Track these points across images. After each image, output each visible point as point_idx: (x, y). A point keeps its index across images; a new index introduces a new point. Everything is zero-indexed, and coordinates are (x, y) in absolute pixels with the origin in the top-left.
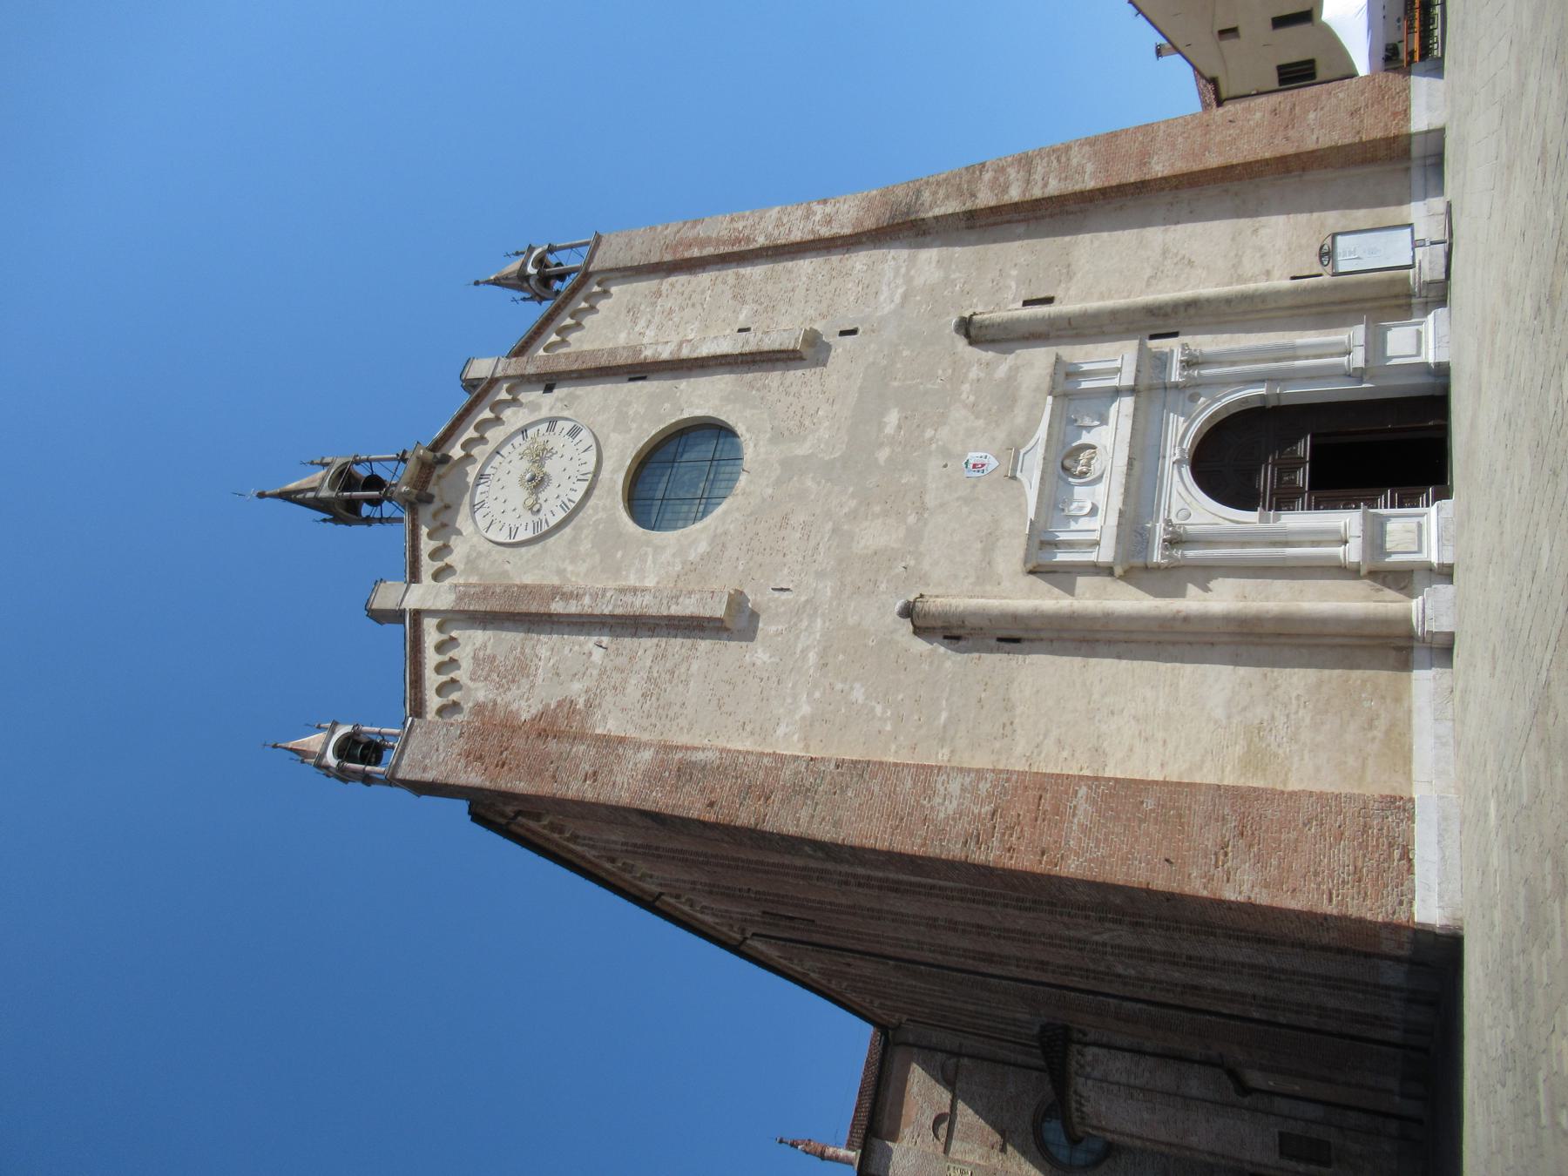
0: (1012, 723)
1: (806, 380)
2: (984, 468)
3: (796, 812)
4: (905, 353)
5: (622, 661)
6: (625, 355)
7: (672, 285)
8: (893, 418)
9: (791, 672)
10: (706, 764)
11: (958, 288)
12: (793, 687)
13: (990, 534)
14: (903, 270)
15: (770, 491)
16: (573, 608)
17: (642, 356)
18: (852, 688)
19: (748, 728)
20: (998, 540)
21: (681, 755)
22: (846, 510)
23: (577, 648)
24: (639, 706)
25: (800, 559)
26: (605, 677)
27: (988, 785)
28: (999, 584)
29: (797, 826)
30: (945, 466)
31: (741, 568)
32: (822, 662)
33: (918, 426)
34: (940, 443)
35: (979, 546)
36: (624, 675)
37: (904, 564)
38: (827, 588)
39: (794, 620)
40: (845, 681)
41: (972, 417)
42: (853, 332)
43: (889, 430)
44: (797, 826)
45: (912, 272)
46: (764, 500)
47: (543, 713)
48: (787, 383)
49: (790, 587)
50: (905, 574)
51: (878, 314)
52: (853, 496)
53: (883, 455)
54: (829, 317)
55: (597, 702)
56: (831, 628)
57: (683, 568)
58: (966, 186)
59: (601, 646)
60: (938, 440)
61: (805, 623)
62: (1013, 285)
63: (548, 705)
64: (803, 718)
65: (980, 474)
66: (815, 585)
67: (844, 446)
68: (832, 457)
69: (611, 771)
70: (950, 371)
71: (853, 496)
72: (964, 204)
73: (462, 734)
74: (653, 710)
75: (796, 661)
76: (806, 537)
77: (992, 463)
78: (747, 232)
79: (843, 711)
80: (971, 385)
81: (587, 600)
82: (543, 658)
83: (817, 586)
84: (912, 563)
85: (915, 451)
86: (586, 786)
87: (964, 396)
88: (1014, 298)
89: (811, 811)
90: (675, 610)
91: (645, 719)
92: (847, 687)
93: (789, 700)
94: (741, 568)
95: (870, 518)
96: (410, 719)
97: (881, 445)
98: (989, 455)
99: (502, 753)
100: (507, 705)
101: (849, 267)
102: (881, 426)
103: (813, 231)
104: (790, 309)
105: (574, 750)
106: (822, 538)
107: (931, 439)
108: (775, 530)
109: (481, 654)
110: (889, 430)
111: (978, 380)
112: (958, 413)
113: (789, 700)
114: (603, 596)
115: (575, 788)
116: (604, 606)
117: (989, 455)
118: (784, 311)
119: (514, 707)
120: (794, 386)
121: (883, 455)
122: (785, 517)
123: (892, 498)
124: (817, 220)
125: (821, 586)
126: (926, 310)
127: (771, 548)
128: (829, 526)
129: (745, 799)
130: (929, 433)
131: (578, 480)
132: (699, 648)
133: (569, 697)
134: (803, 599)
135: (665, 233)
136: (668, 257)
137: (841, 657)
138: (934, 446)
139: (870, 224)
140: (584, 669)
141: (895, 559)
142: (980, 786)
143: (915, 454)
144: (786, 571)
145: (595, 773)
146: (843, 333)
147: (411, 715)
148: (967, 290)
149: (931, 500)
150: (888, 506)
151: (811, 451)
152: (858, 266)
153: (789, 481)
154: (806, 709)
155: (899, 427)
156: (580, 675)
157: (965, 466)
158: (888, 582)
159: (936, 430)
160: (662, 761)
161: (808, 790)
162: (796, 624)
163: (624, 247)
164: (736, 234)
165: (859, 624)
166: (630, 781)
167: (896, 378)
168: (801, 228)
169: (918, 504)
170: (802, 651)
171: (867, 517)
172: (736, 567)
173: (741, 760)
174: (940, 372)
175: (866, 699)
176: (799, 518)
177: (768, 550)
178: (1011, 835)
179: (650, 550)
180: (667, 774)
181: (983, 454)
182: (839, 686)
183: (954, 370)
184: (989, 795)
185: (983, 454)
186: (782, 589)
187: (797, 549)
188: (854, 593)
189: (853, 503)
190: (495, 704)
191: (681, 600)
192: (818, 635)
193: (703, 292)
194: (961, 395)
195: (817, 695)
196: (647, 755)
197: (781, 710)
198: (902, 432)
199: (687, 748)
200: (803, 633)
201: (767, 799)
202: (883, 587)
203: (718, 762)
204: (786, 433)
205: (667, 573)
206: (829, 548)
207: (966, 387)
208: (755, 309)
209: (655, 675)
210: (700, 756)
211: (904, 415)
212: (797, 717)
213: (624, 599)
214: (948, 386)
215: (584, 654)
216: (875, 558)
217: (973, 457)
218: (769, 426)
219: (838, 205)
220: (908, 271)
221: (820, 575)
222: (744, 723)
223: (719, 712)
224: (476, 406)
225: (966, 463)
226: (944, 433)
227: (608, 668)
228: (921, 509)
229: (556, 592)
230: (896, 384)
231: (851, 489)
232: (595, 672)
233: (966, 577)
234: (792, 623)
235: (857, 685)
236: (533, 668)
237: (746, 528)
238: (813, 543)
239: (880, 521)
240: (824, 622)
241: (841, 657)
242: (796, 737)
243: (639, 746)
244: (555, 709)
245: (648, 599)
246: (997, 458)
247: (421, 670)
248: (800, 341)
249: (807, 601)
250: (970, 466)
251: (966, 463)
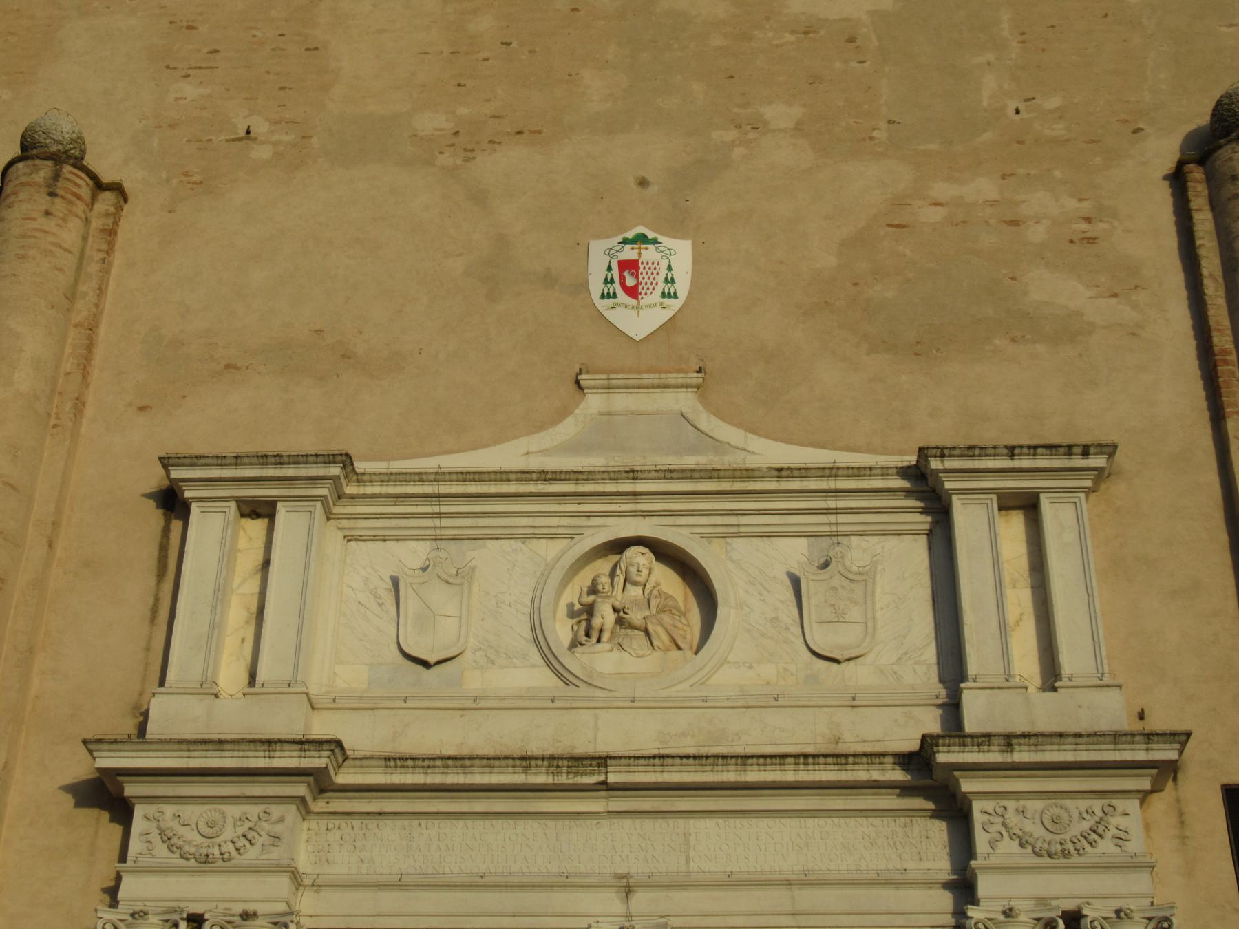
2: (622, 297)
28: (142, 409)
30: (643, 183)
37: (260, 127)
65: (596, 286)
87: (942, 190)
98: (676, 304)
111: (1014, 223)
130: (780, 114)
157: (630, 235)
181: (683, 286)
202: (190, 90)
225: (642, 239)
250: (629, 253)
251: (642, 239)
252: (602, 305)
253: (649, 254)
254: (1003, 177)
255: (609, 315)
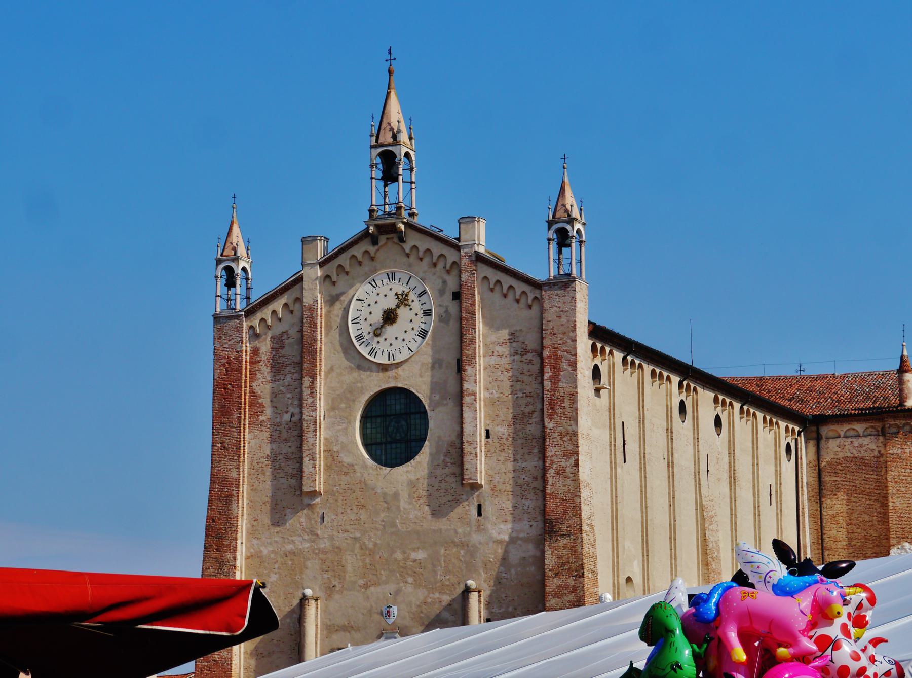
0: (263, 657)
1: (449, 490)
2: (388, 617)
3: (212, 567)
4: (462, 552)
5: (284, 435)
6: (469, 353)
7: (531, 361)
8: (420, 555)
9: (282, 538)
10: (231, 510)
11: (504, 575)
12: (276, 542)
13: (352, 628)
14: (522, 535)
15: (379, 491)
16: (306, 392)
17: (467, 367)
18: (276, 573)
19: (255, 524)
20: (349, 632)
21: (235, 494)
22: (367, 542)
23: (290, 401)
24: (263, 455)
25: (340, 524)
26: (275, 427)
27: (226, 656)
29: (206, 569)
31: (335, 489)
32: (287, 553)
33: (415, 572)
34: (404, 588)
35: (346, 623)
36: (278, 439)
38: (324, 544)
39: (306, 530)
40: (279, 568)
41: (418, 603)
42: (480, 514)
43: (414, 555)
44: (206, 569)
45: (519, 542)
46: (373, 489)
47: (256, 396)
48: (448, 479)
49: (325, 522)
50: (331, 586)
51: (490, 527)
52: (375, 545)
53: (399, 555)
54: (492, 493)
55: (263, 428)
56: (304, 553)
57: (335, 452)
58: (567, 568)
59: (291, 417)
60: (405, 586)
61: (306, 537)
62: (503, 610)
63: (260, 398)
64: (261, 551)
66: (326, 537)
67: (405, 530)
68: (398, 524)
69: (226, 456)
70: (447, 583)
71: (375, 545)
72: (549, 570)
73: (237, 352)
74: (261, 464)
75: (288, 539)
76: (352, 523)
77: (391, 621)
78: (559, 411)
79: (265, 572)
80: (438, 598)
81: (310, 400)
82: (285, 381)
83: (326, 538)
84: (337, 589)
85: (400, 575)
86: (218, 445)
87: (431, 595)
88: (492, 612)
89: (213, 574)
90: (306, 460)
91: (256, 462)
92: (276, 570)
93: (269, 541)
94: (335, 489)
95: (362, 558)
96: (243, 313)
97: (404, 553)
98: (395, 618)
99: (230, 384)
100: (259, 370)
101: (529, 496)
102: (414, 550)
103: (552, 462)
104: (500, 463)
105: (234, 429)
106: (351, 533)
107: (406, 582)
108: (356, 503)
109: (285, 337)
110: (414, 555)
111: (440, 602)
112: (421, 594)
113: (269, 541)
114: (312, 410)
115: (217, 439)
116: (307, 414)
117: (395, 618)
118: (499, 458)
119: (259, 375)
120: (446, 484)
121: (399, 555)
122: (363, 506)
123: (373, 568)
124: (563, 464)
125: (326, 540)
126: (490, 558)
127: (346, 504)
128: (358, 535)
129: (216, 538)
130: (410, 580)
131: (389, 353)
132: (292, 480)
133: (264, 409)
134: (319, 532)
135: (569, 341)
136: (546, 353)
137: (290, 563)
138: (402, 584)
139: (551, 505)
140: (279, 412)
141: (340, 579)
142: (225, 652)
143: (398, 575)
144: (334, 517)
145: (224, 448)
146: (480, 506)
147: (245, 312)
148: (501, 581)
149: (372, 589)
150: (369, 567)
151: (402, 509)
152: (527, 503)
153: (385, 501)
154: (265, 552)
155: (415, 561)
156: (276, 411)
158: (328, 578)
159: (412, 583)
160: (232, 484)
161: (221, 569)
162: (306, 532)
163: (561, 309)
164: (560, 403)
165: (307, 568)
166: (222, 470)
167: (446, 550)
168: (557, 453)
169: (369, 583)
170: (292, 541)
171: (362, 556)
172: (335, 486)
173: (233, 529)
174: (448, 577)
175: (271, 582)
176: (363, 515)
177: (345, 502)
178: (207, 670)
179: (344, 426)
180: (226, 490)
181: (396, 615)
182: (276, 566)
183: (448, 585)
184: (222, 657)
185: (396, 615)
186: (323, 518)
187: (345, 521)
188: (322, 561)
189: (371, 546)
190: (259, 362)
191: (311, 462)
192: (301, 547)
193: (521, 390)
194: (433, 593)
195: (272, 556)
196: (234, 474)
197: (264, 538)
198: (411, 563)
199: (238, 496)
200: (301, 538)
201: (217, 550)
202: (325, 576)
203: (232, 517)
204: (414, 490)
205: (332, 442)
206: (346, 539)
207: (437, 595)
208: (503, 436)
209: (278, 459)
210: (234, 506)
211: (422, 562)
212: (262, 549)
213: (311, 425)
214: (438, 584)
215: (287, 408)
216: (340, 567)
217: (394, 609)
218: (418, 476)
219: (572, 475)
220: (521, 539)
221: (332, 538)
222: (257, 520)
223: (262, 503)
224: (442, 243)
225: (390, 607)
226: (409, 589)
227: (280, 427)
228: (366, 586)
229: (314, 377)
230: (442, 551)
231: (378, 542)
232: (278, 420)
233: (330, 620)
234: (306, 530)
235: (277, 576)
236: (278, 377)
237: (357, 484)
238: (348, 528)
239: (361, 564)
240: (307, 548)
241: (290, 563)
242: (252, 550)
243: (238, 468)
244: (258, 403)
245: (311, 440)
246: (394, 623)
247: (271, 301)
248: (471, 481)
249: (317, 535)
250: (388, 609)
251: (390, 607)
252: (385, 618)
253: (391, 609)
254: (440, 592)
255: (386, 620)
